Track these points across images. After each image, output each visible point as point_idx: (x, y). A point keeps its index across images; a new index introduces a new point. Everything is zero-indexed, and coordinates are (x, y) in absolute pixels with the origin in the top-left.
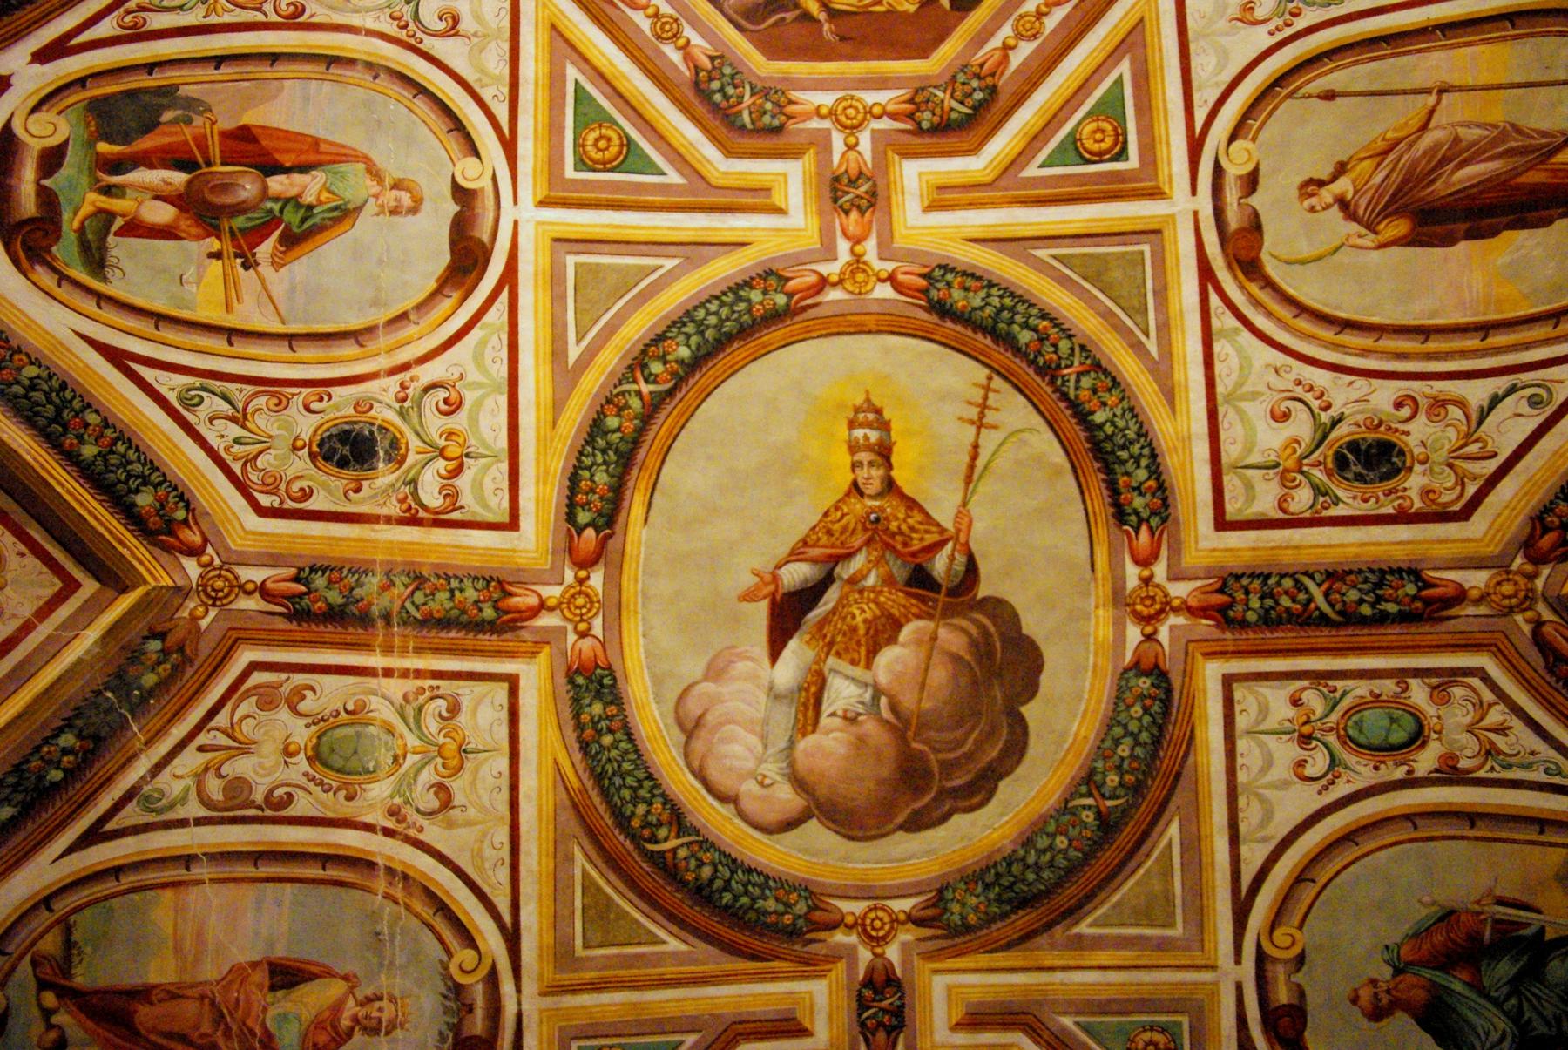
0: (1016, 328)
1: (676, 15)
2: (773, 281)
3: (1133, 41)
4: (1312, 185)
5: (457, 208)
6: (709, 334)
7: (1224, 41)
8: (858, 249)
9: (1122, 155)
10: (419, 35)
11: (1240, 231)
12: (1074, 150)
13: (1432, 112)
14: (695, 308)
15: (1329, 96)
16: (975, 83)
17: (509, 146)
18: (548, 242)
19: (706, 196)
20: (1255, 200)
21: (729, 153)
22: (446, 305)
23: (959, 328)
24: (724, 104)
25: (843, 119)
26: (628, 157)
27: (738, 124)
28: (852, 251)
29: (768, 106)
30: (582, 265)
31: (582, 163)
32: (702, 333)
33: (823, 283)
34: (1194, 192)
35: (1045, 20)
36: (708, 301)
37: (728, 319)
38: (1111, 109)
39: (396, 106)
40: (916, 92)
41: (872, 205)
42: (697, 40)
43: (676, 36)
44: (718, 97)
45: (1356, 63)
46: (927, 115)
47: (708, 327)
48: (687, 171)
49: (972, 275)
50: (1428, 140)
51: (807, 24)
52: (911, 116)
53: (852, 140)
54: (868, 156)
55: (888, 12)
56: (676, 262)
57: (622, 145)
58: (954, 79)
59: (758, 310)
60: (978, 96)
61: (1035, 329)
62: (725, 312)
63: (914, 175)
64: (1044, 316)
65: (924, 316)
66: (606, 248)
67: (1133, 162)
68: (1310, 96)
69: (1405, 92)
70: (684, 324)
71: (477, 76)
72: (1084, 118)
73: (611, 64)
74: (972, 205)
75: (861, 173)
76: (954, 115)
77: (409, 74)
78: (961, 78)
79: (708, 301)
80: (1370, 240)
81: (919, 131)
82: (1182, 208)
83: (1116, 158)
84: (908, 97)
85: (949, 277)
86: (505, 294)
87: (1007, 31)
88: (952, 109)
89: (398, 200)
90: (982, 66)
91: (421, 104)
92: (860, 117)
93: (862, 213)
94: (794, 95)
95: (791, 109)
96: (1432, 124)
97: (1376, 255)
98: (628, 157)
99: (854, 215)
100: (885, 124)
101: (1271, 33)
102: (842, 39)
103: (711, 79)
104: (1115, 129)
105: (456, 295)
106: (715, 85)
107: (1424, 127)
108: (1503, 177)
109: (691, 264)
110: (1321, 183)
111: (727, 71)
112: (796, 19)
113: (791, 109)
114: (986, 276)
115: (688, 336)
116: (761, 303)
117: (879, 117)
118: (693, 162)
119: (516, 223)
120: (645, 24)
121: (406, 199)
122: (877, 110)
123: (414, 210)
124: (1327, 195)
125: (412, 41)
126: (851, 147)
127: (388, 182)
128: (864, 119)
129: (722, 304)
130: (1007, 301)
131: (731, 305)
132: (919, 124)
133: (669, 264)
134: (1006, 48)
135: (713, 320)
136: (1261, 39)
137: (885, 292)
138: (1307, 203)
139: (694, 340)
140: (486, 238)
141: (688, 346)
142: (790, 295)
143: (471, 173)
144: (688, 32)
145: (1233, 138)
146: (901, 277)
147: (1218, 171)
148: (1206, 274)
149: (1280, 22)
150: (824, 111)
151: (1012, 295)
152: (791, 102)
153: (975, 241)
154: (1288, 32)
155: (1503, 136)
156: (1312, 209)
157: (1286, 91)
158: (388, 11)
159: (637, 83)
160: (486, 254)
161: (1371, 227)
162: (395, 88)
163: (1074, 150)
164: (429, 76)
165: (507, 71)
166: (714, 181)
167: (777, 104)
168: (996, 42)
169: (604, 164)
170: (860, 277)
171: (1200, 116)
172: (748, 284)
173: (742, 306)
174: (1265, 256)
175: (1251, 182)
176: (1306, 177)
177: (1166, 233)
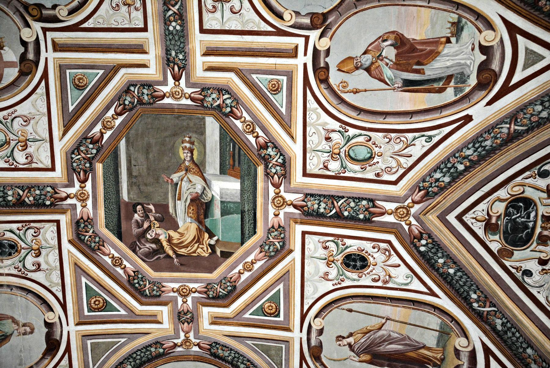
0: (239, 363)
1: (120, 257)
2: (158, 345)
3: (285, 277)
4: (340, 338)
5: (47, 330)
6: (138, 361)
7: (317, 284)
8: (187, 335)
9: (278, 315)
10: (26, 272)
11: (315, 346)
12: (262, 311)
13: (383, 325)
14: (132, 354)
15: (350, 311)
16: (228, 284)
17: (64, 306)
18: (80, 337)
19: (133, 318)
20: (321, 338)
21: (142, 304)
22: (46, 361)
23: (220, 361)
24: (139, 288)
25: (182, 293)
26: (106, 306)
27: (145, 294)
28: (185, 335)
29: (155, 288)
30: (93, 343)
31: (90, 310)
32: (135, 361)
33: (175, 345)
34: (301, 331)
35: (254, 265)
36: (137, 351)
37: (143, 357)
38: (275, 299)
39: (20, 299)
40: (208, 285)
41: (192, 321)
42: (128, 265)
43: (121, 264)
44: (137, 285)
45: (360, 302)
46: (211, 293)
47: (137, 359)
48: (127, 310)
49: (225, 346)
50: (381, 333)
51: (168, 259)
52: (206, 293)
53: (185, 300)
54: (191, 306)
55: (198, 256)
56: (125, 339)
57: (104, 303)
58: (221, 281)
59: (154, 354)
60: (229, 288)
61: (245, 364)
62: (142, 355)
63: (206, 311)
64: (249, 361)
65: (209, 357)
66: (101, 337)
67: (281, 318)
68: (344, 309)
69: (375, 316)
70: (129, 359)
71: (49, 284)
72: (266, 301)
73: (98, 276)
74: (226, 324)
75: (188, 311)
76: (221, 294)
77: (24, 287)
78: (223, 281)
79: (137, 351)
80: (357, 359)
81: (208, 298)
82: (297, 336)
83: (276, 316)
84: (205, 286)
85: (218, 346)
86: (67, 355)
87: (240, 267)
88: (220, 292)
89: (25, 330)
90: (231, 278)
91: (30, 296)
92: (188, 292)
93: (189, 323)
94: (164, 284)
95: (163, 289)
96: (382, 329)
97: (358, 364)
98: (106, 306)
99: (186, 324)
100: (196, 295)
101: (333, 285)
102: (181, 265)
103: (134, 279)
104: (276, 307)
105: (49, 358)
106: (136, 281)
107: (380, 329)
108: (403, 351)
109: (130, 340)
110: (344, 338)
111: (140, 276)
112: (164, 257)
113: (163, 289)
114: (230, 347)
115: (131, 362)
116: (155, 352)
117: (195, 292)
118: (129, 307)
119: (69, 332)
120: (109, 261)
121: (28, 329)
122: (193, 290)
123: (32, 332)
124: (345, 342)
125: (24, 275)
126: (184, 302)
127: (21, 324)
128: (189, 293)
129: (142, 352)
130: (237, 355)
131: (145, 353)
132: (208, 295)
133: (123, 340)
134: (240, 273)
135: (139, 357)
136: (329, 286)
137: (196, 349)
138: (338, 343)
139: (132, 363)
140: (58, 338)
141: (130, 365)
142: (164, 349)
143: (51, 317)
144: (125, 262)
145: (316, 317)
146: (201, 345)
147: (310, 326)
148: (302, 357)
149: (337, 282)
150: (175, 290)
151: (238, 353)
152: (163, 287)
153: (226, 336)
154: (339, 286)
155: (404, 339)
156: (340, 345)
157: (336, 306)
158: (13, 266)
159: (107, 282)
160: (59, 343)
161: (358, 355)
162: (19, 292)
163: (262, 311)
164: (32, 286)
165: (60, 281)
166: (137, 313)
167: (158, 287)
168: (236, 271)
169: (98, 309)
170: (188, 344)
171: (306, 308)
172: (150, 346)
173: (148, 352)
174: (322, 355)
175: (321, 332)
176: (339, 334)
177: (290, 343)
